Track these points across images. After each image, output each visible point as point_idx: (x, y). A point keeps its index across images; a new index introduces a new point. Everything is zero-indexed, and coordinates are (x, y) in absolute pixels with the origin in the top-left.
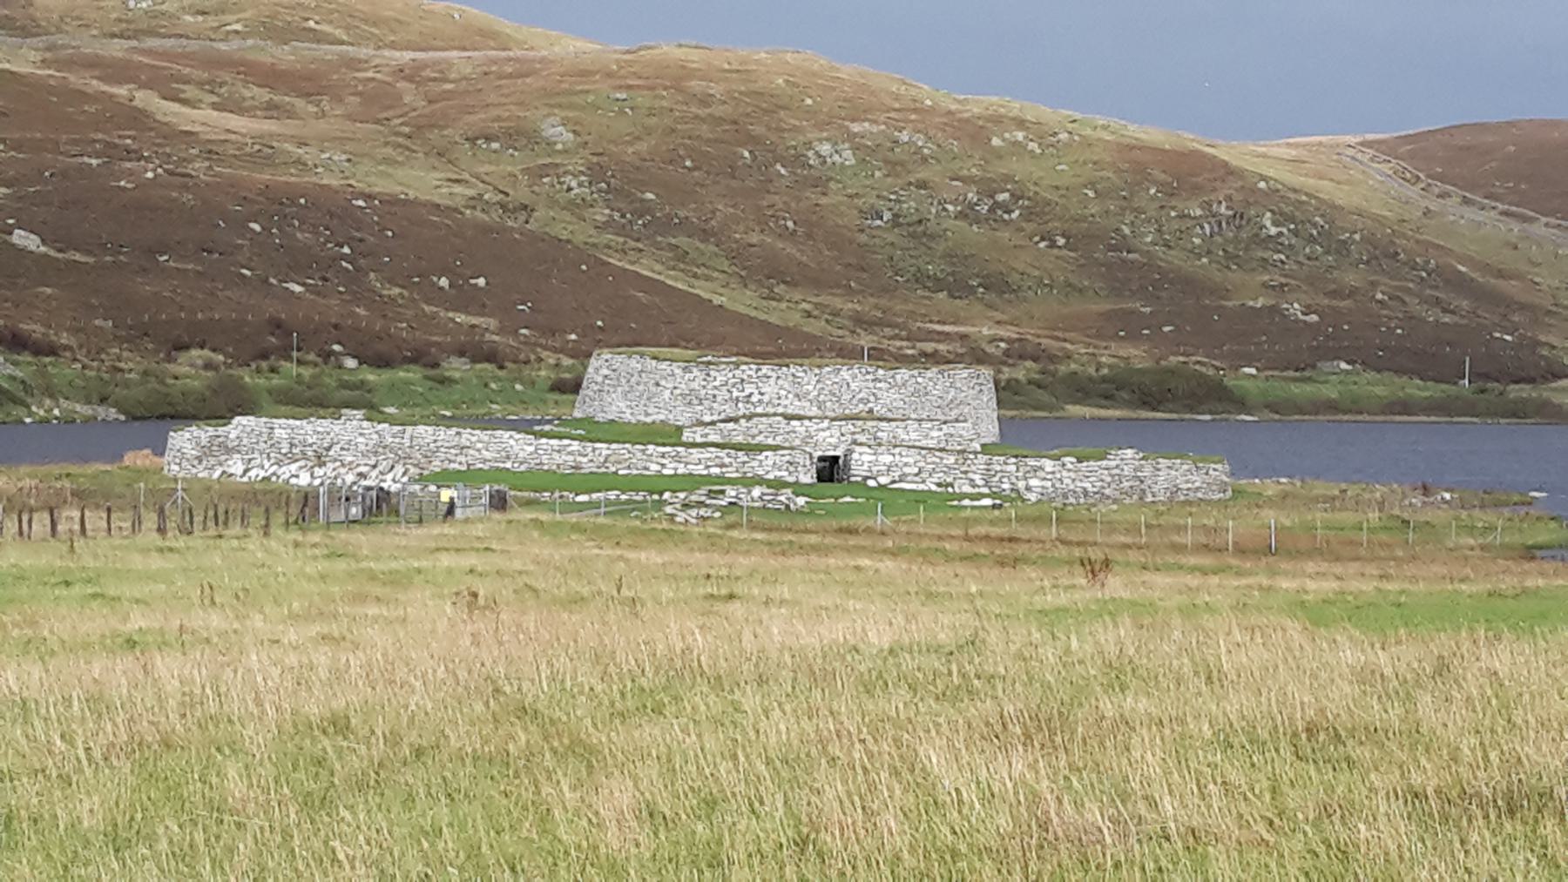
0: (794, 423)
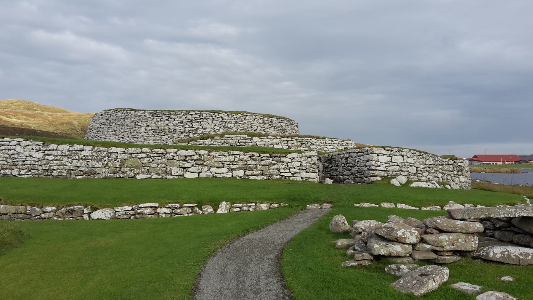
0: (254, 138)
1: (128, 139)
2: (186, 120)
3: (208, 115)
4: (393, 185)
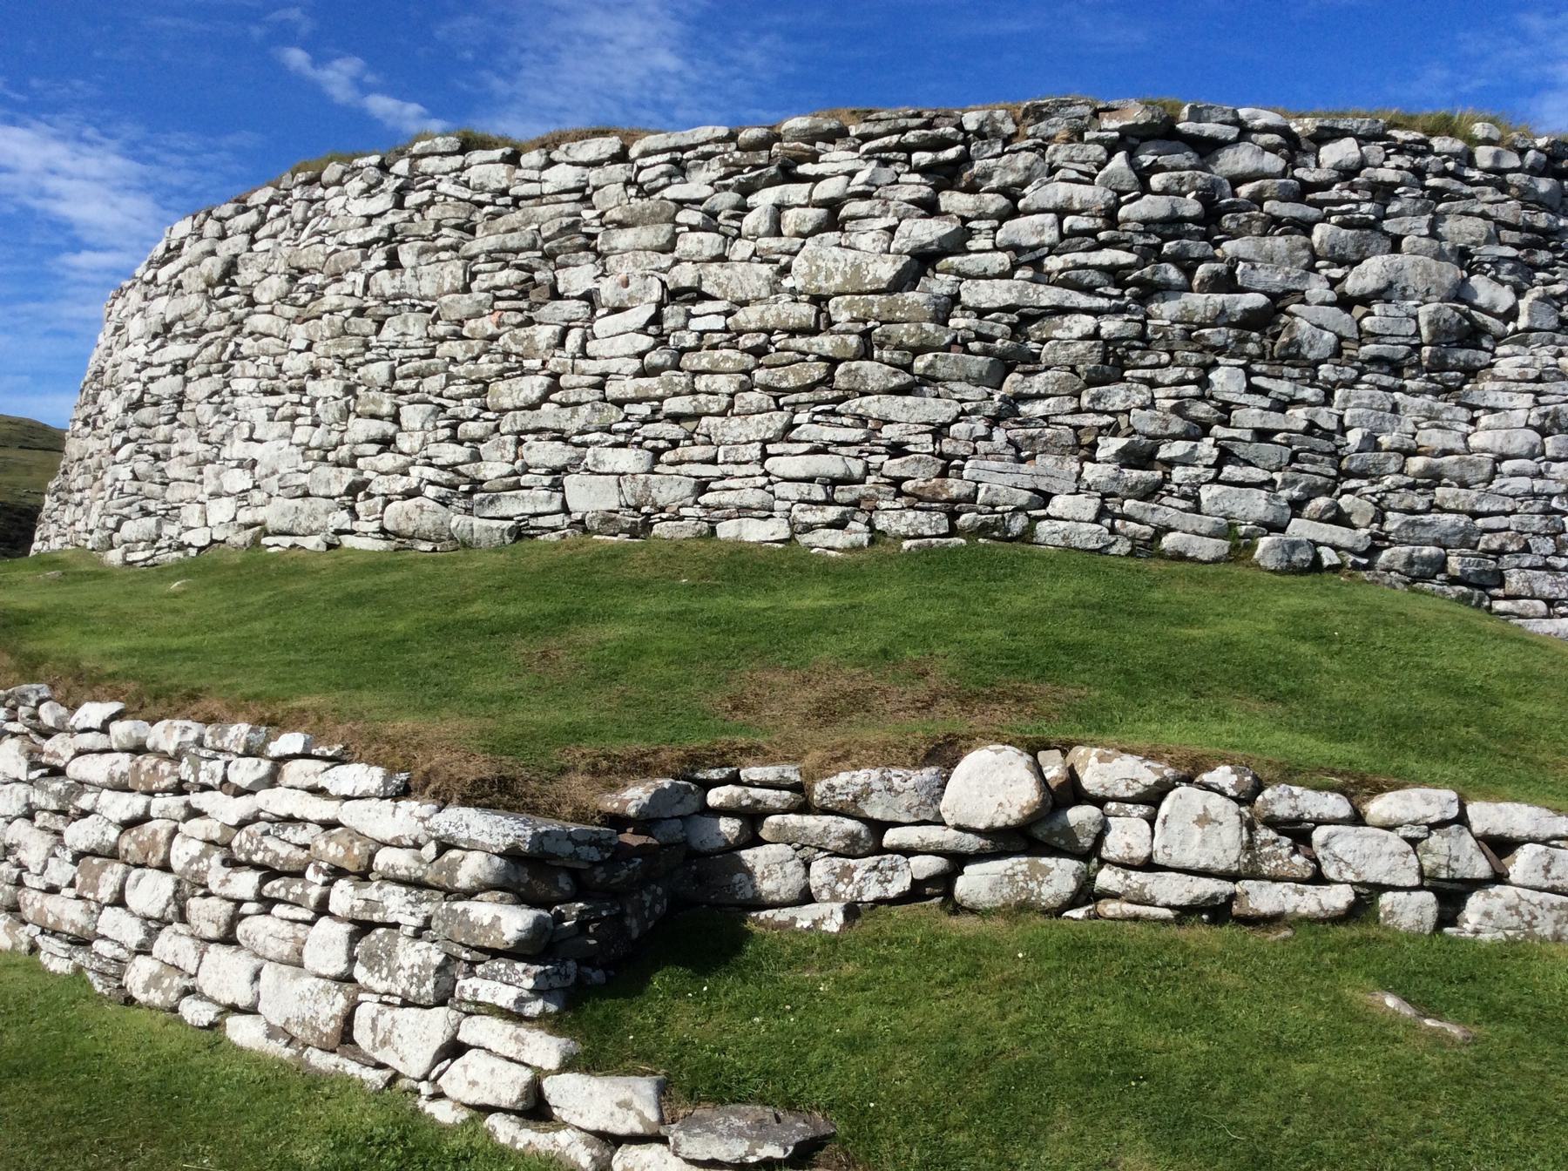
1: (452, 453)
2: (1150, 207)
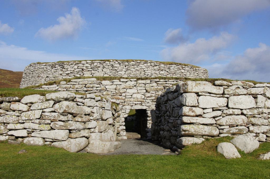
0: (104, 82)
3: (99, 64)
4: (222, 156)
